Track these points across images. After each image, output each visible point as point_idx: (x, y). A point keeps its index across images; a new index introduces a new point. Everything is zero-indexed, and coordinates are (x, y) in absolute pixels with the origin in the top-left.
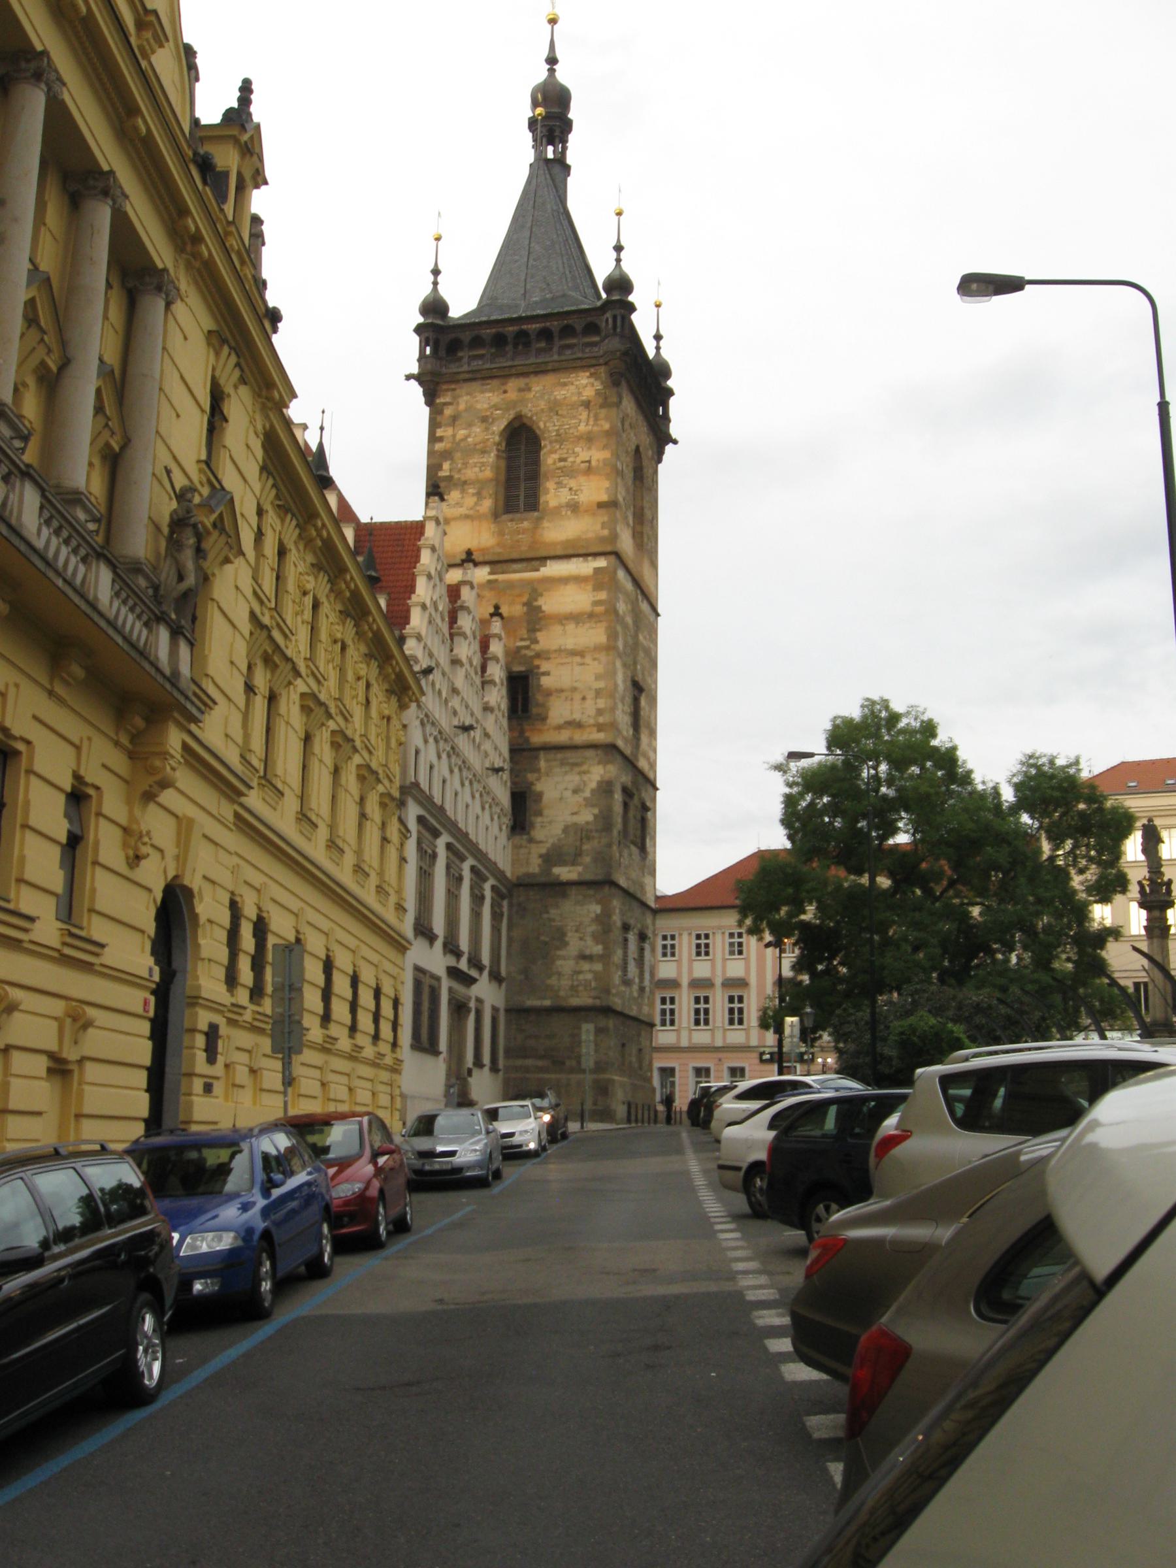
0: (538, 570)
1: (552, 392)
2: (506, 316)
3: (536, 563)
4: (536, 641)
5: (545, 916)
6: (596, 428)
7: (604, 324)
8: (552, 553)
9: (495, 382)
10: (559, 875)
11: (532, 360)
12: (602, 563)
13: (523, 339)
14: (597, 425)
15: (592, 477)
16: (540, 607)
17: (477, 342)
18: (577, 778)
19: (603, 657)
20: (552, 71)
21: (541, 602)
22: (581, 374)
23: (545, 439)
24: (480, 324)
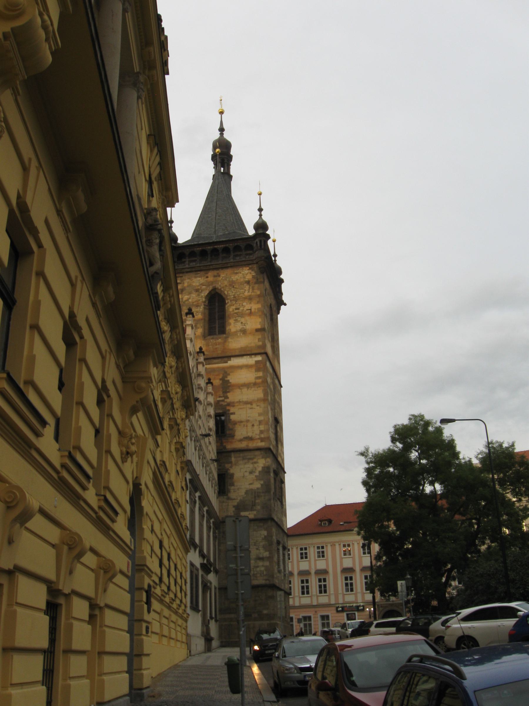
0: (227, 362)
1: (231, 277)
2: (207, 242)
3: (226, 359)
4: (227, 398)
6: (253, 294)
7: (255, 245)
8: (234, 354)
9: (202, 273)
11: (220, 262)
12: (259, 358)
13: (215, 252)
14: (254, 292)
15: (252, 317)
16: (228, 381)
17: (192, 254)
18: (251, 466)
19: (262, 405)
20: (222, 134)
21: (229, 378)
22: (244, 268)
23: (228, 299)
24: (194, 245)
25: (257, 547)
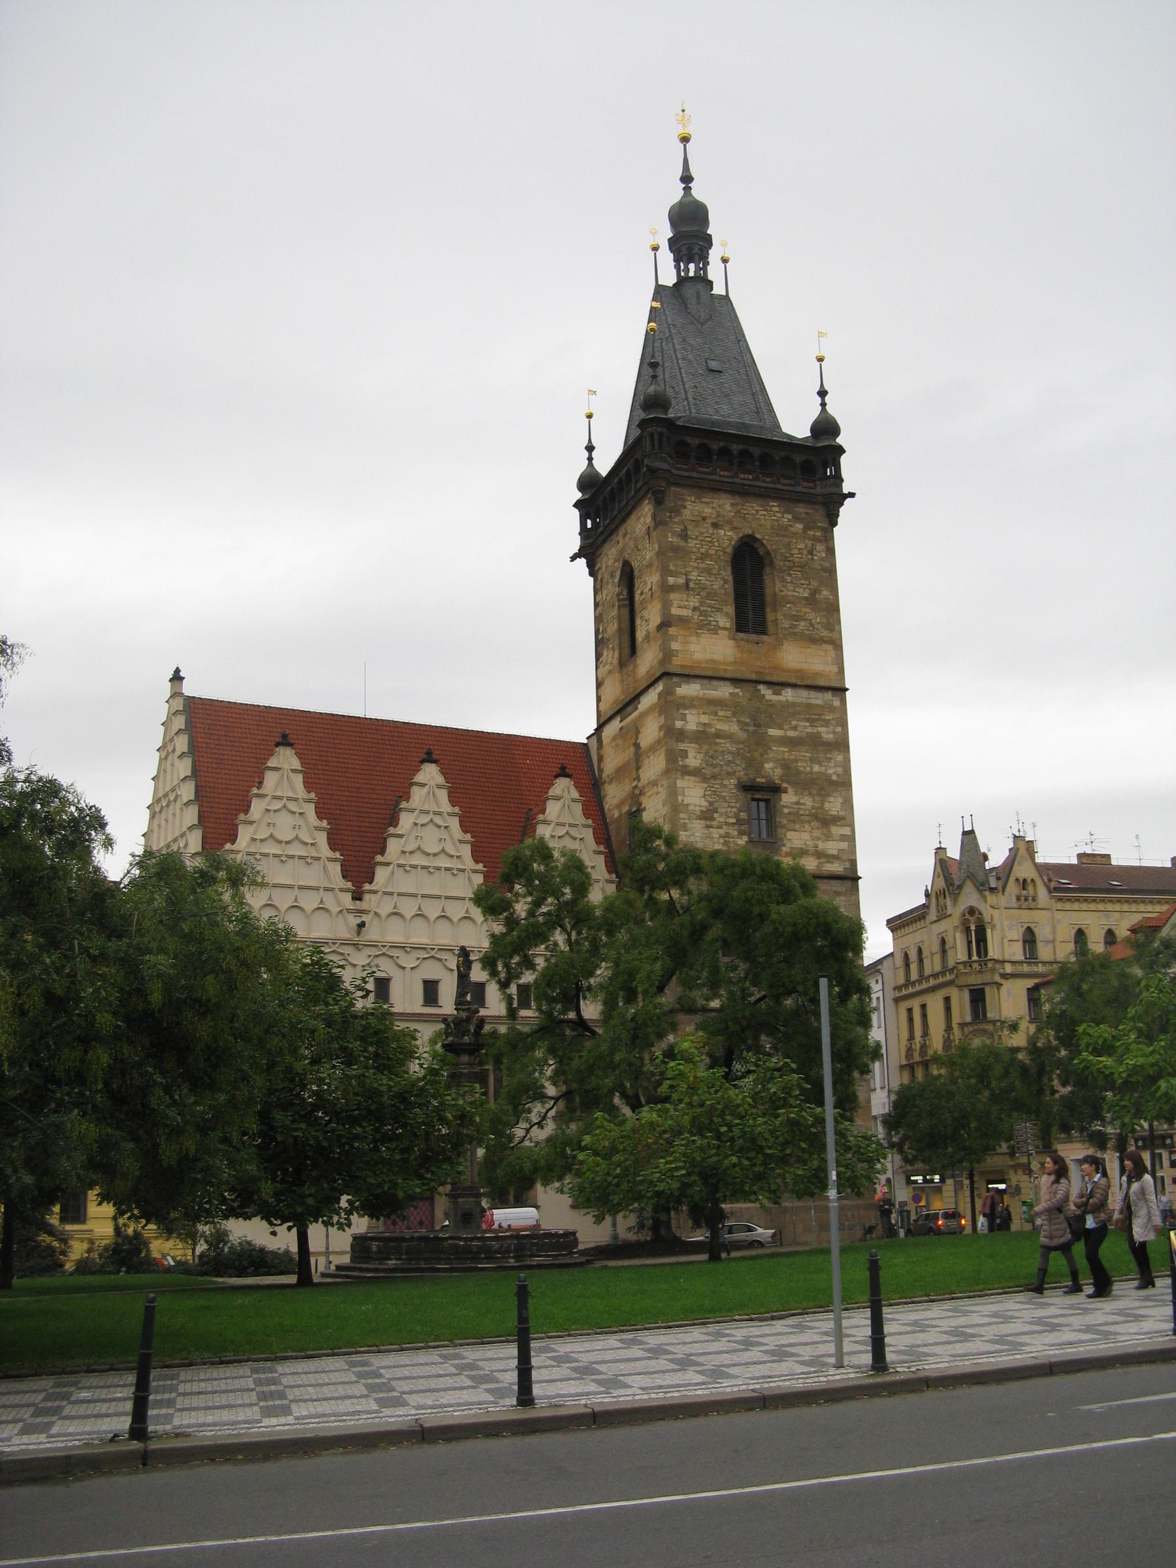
0: (637, 709)
12: (660, 687)
20: (687, 189)
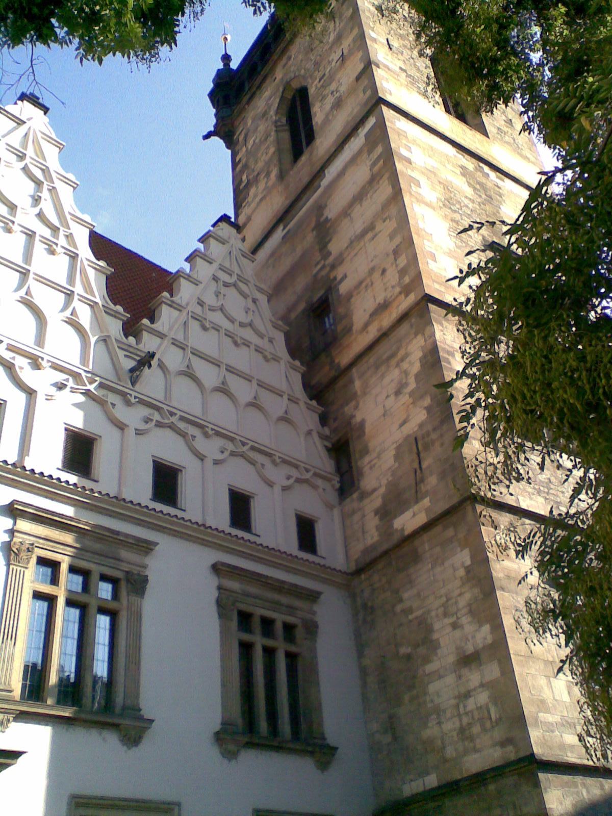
0: (319, 186)
5: (399, 608)
10: (403, 530)
25: (453, 619)
